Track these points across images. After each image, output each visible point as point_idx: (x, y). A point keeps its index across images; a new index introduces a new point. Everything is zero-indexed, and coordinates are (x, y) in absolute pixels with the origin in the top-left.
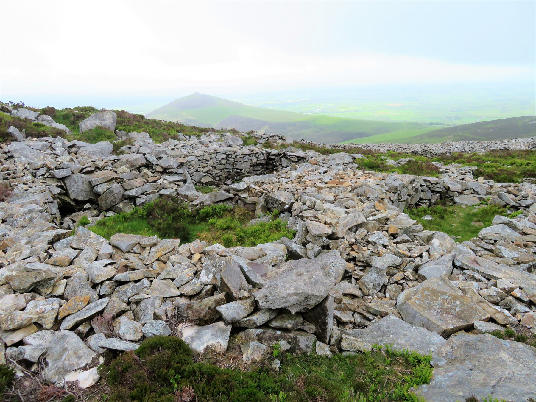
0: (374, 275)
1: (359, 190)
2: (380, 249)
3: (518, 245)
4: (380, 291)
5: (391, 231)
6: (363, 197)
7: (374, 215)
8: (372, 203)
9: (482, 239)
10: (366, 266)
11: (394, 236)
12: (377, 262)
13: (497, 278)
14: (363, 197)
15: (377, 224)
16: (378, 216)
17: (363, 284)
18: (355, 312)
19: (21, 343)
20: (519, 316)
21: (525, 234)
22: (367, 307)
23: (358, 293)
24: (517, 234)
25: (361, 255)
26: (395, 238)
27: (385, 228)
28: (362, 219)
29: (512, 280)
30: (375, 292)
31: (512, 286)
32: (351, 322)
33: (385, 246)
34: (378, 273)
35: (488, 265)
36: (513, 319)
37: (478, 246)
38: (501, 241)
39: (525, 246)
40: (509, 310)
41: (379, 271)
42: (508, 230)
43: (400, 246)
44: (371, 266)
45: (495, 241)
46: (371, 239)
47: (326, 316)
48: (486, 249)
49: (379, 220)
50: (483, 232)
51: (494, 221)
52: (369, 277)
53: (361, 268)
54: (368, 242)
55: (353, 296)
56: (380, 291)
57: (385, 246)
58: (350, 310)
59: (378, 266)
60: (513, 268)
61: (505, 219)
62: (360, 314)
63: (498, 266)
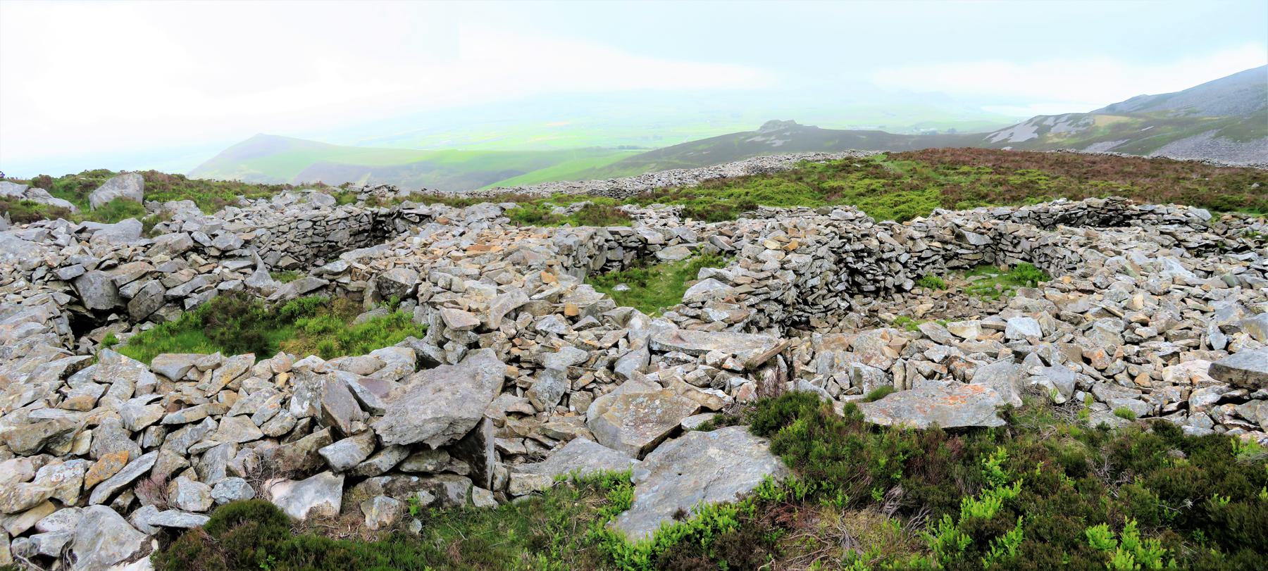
0: (550, 381)
1: (515, 256)
2: (555, 340)
3: (729, 301)
4: (560, 404)
5: (568, 312)
6: (522, 266)
7: (540, 292)
8: (537, 274)
9: (687, 305)
10: (537, 368)
11: (573, 319)
12: (552, 361)
13: (706, 352)
14: (522, 266)
15: (547, 304)
16: (547, 293)
17: (534, 394)
18: (525, 438)
19: (33, 531)
20: (734, 393)
21: (737, 285)
22: (543, 429)
23: (527, 409)
24: (728, 288)
25: (527, 353)
26: (575, 322)
27: (559, 309)
28: (524, 299)
29: (724, 349)
30: (554, 405)
31: (724, 356)
32: (522, 454)
33: (561, 336)
34: (555, 377)
35: (695, 338)
36: (728, 399)
37: (682, 315)
38: (710, 302)
39: (738, 300)
40: (723, 389)
41: (555, 373)
42: (717, 284)
43: (583, 333)
44: (543, 368)
45: (703, 303)
46: (538, 328)
47: (483, 447)
48: (692, 317)
49: (549, 298)
50: (688, 294)
51: (700, 276)
52: (542, 384)
53: (529, 372)
54: (536, 332)
55: (521, 415)
56: (560, 404)
57: (561, 336)
58: (519, 436)
59: (554, 366)
60: (726, 332)
61: (712, 270)
62: (534, 440)
63: (707, 335)
